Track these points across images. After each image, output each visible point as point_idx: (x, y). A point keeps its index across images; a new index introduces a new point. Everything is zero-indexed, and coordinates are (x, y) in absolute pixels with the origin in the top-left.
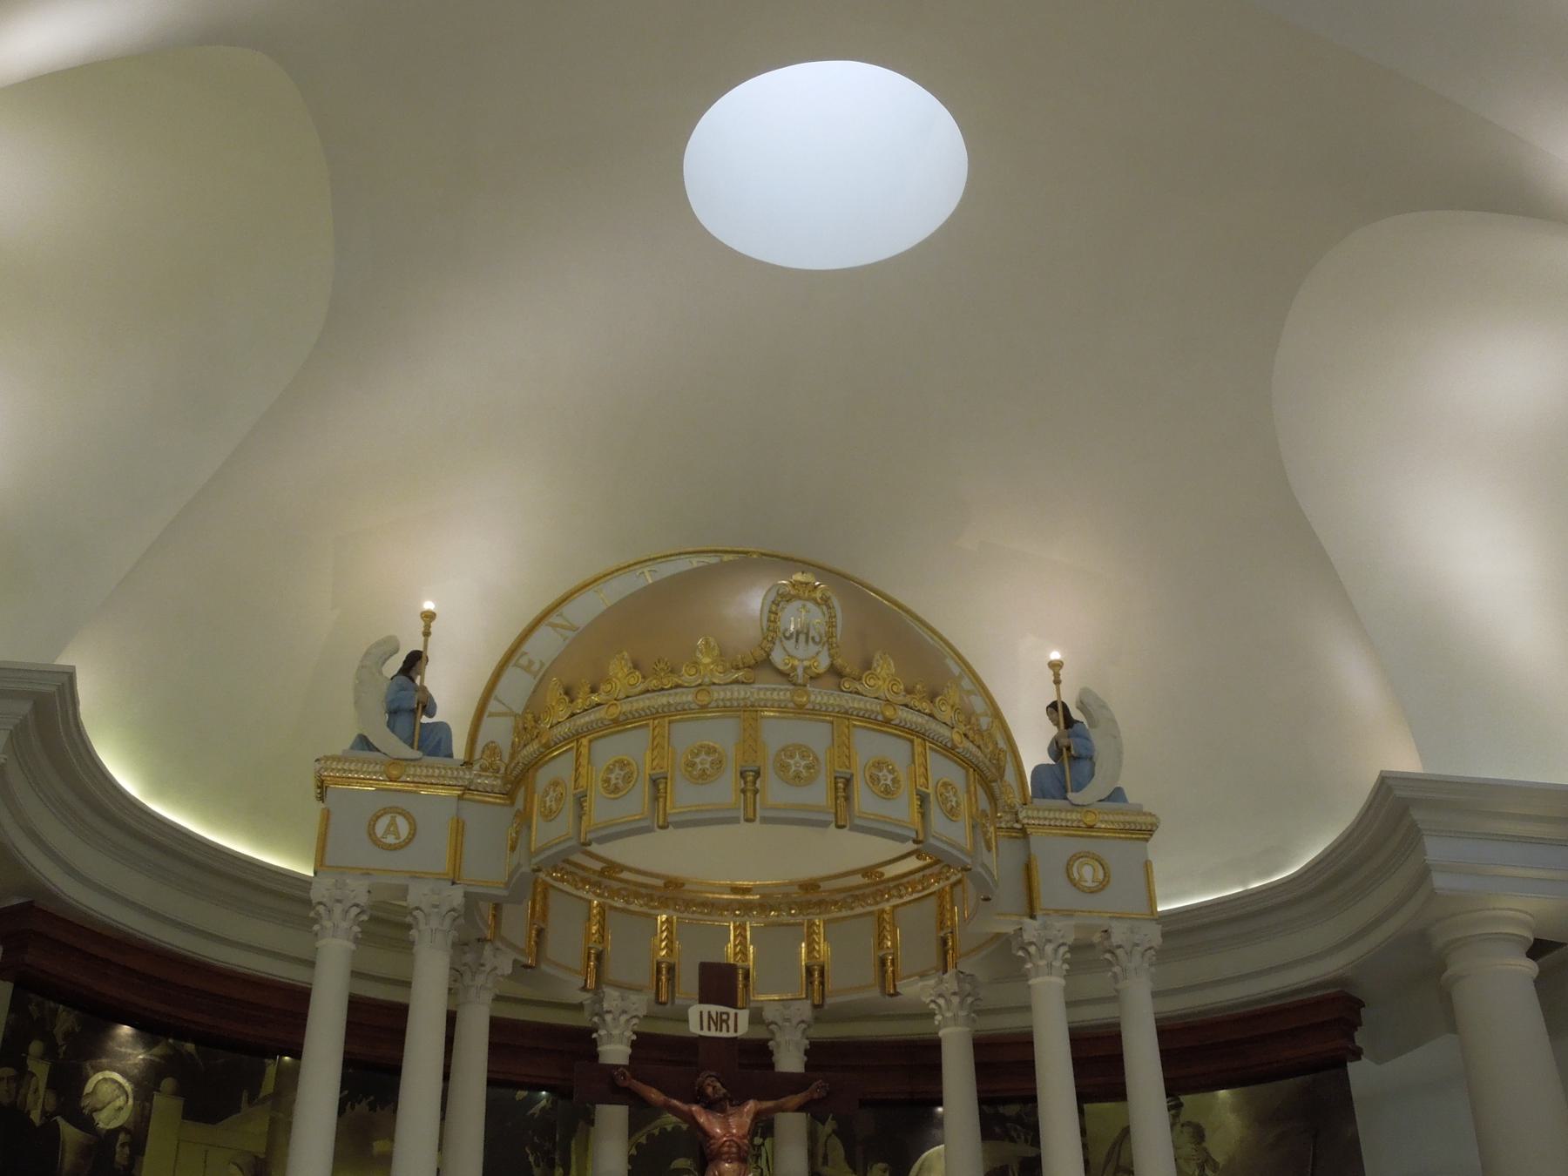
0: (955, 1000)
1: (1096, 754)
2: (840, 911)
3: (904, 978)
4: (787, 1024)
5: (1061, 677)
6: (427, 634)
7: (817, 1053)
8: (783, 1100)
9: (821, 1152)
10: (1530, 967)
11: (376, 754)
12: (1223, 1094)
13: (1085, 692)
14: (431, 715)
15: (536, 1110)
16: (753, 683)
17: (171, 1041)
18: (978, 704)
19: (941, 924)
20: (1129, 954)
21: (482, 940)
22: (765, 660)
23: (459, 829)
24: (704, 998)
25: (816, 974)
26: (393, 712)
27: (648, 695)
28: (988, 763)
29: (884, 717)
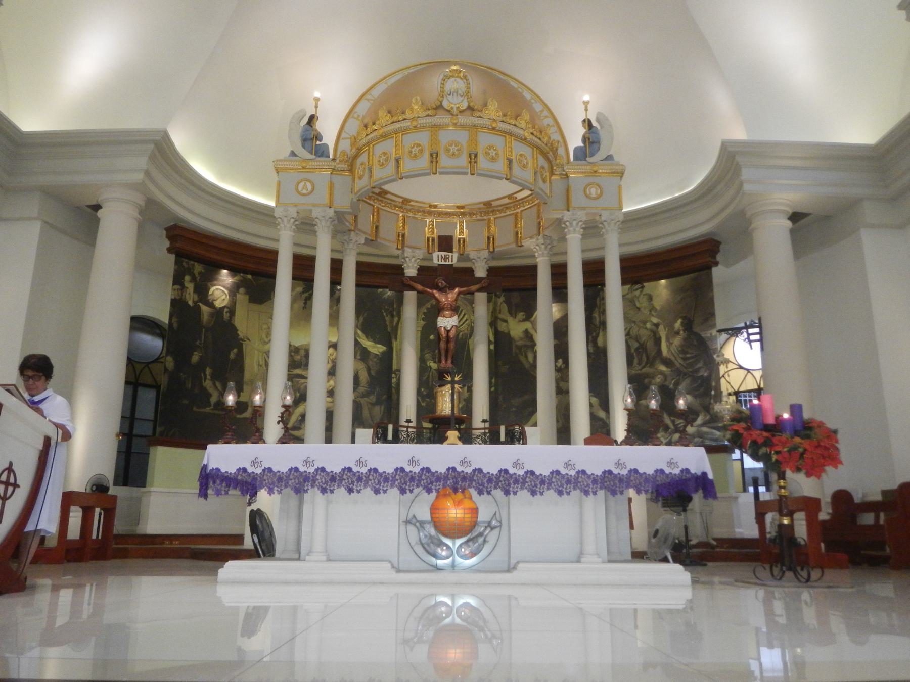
0: (543, 247)
1: (601, 141)
2: (501, 214)
3: (524, 239)
4: (479, 259)
5: (588, 108)
6: (316, 107)
7: (491, 271)
8: (470, 288)
9: (498, 309)
10: (789, 224)
11: (297, 158)
12: (663, 282)
14: (320, 141)
15: (386, 296)
16: (435, 115)
17: (242, 275)
20: (609, 224)
21: (350, 230)
22: (439, 106)
23: (332, 186)
24: (440, 250)
25: (491, 239)
27: (394, 124)
28: (543, 145)
29: (492, 127)
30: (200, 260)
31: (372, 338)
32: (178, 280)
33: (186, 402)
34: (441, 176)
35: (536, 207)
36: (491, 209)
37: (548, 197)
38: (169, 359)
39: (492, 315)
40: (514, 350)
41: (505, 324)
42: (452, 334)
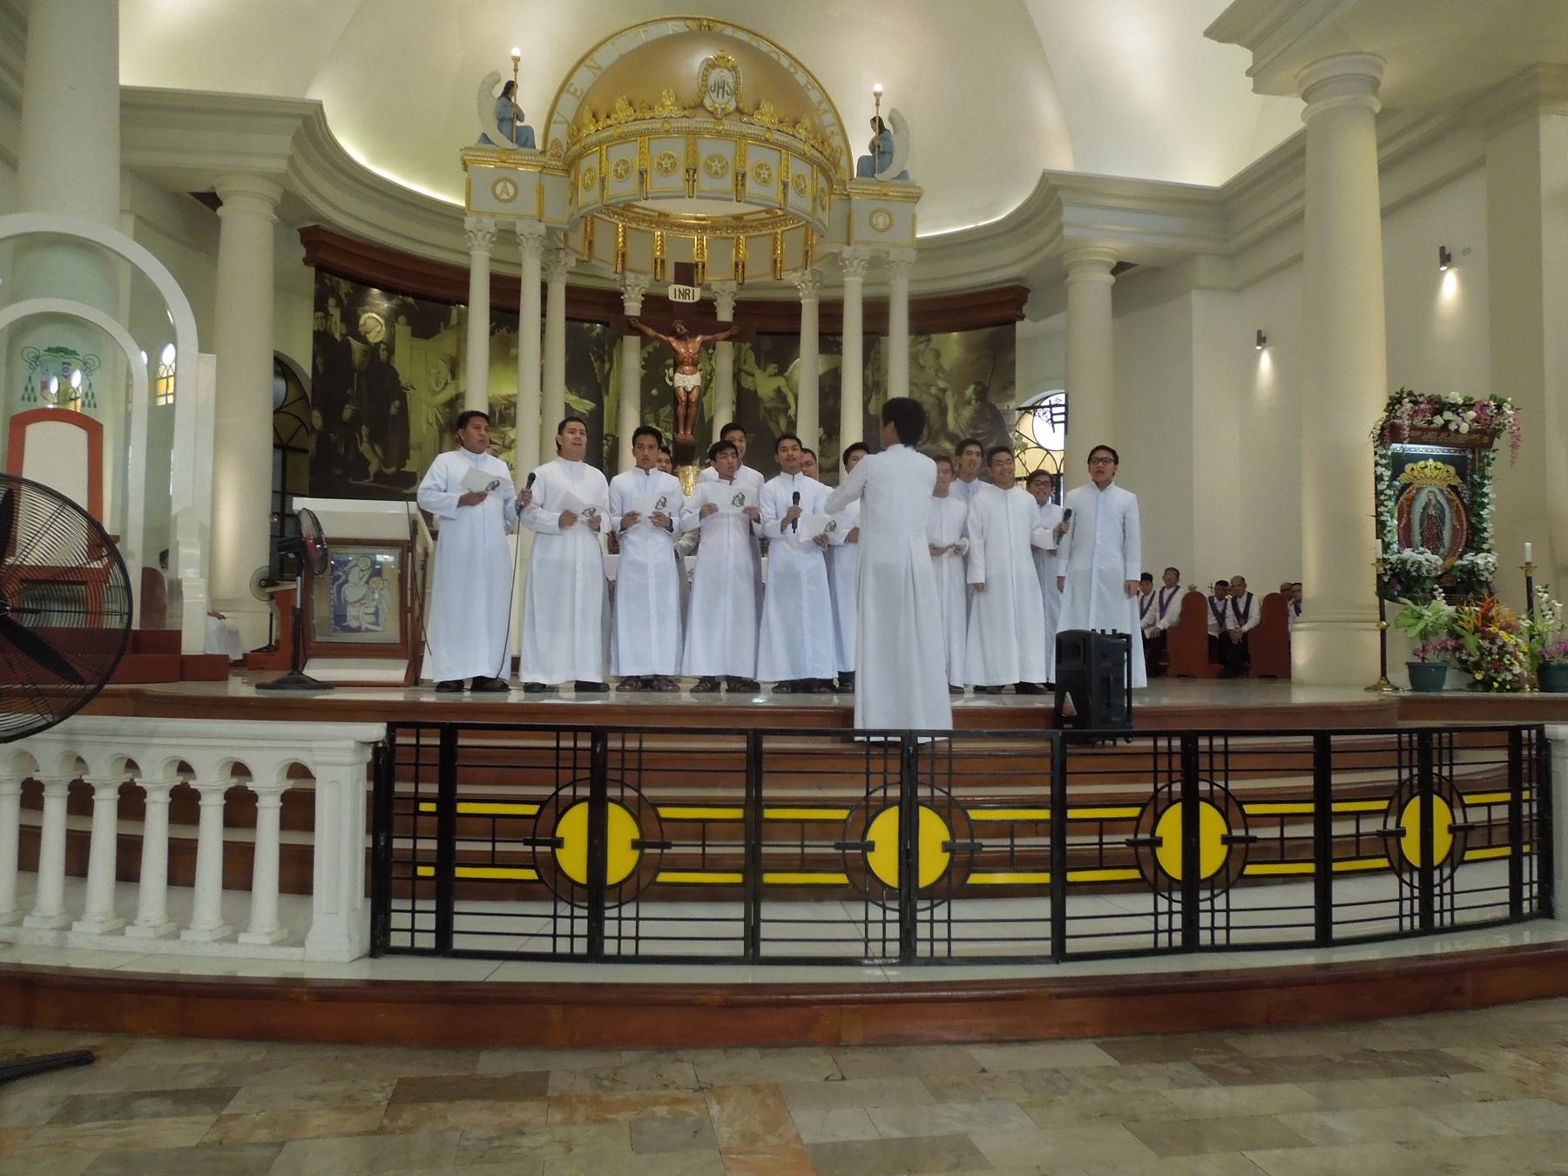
6: (516, 70)
7: (741, 308)
9: (743, 359)
10: (1111, 279)
12: (955, 334)
13: (893, 111)
14: (522, 121)
15: (595, 333)
18: (828, 119)
19: (806, 242)
23: (541, 191)
24: (676, 283)
26: (501, 120)
28: (825, 161)
30: (346, 276)
31: (576, 391)
32: (320, 306)
33: (338, 471)
34: (699, 201)
35: (803, 229)
36: (742, 224)
37: (827, 229)
38: (316, 413)
39: (734, 367)
40: (761, 415)
41: (750, 378)
42: (693, 397)
